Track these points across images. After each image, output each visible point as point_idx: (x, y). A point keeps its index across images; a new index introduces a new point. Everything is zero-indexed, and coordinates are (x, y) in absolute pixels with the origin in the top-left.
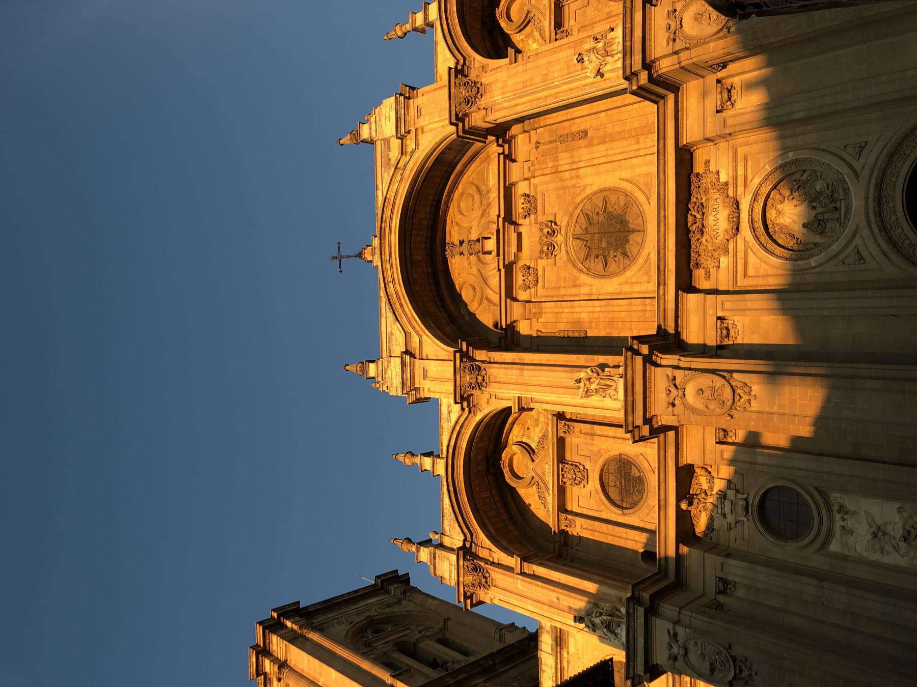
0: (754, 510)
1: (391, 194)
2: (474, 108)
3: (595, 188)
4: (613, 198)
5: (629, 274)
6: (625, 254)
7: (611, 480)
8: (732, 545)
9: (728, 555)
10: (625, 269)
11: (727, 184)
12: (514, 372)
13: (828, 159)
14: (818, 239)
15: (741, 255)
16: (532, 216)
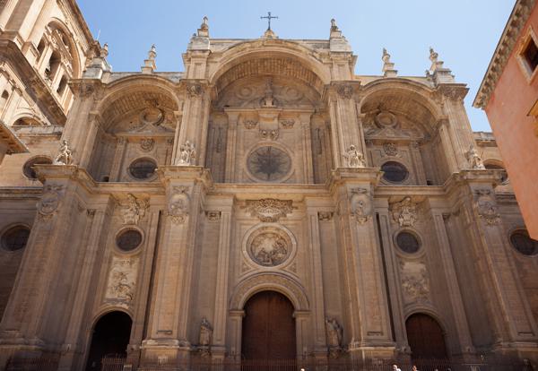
0: (128, 227)
1: (299, 47)
2: (337, 95)
3: (292, 158)
4: (286, 166)
5: (248, 173)
6: (258, 171)
7: (146, 164)
8: (114, 217)
9: (106, 214)
10: (250, 171)
11: (285, 216)
12: (195, 112)
13: (290, 258)
14: (256, 254)
15: (249, 222)
16: (281, 125)
